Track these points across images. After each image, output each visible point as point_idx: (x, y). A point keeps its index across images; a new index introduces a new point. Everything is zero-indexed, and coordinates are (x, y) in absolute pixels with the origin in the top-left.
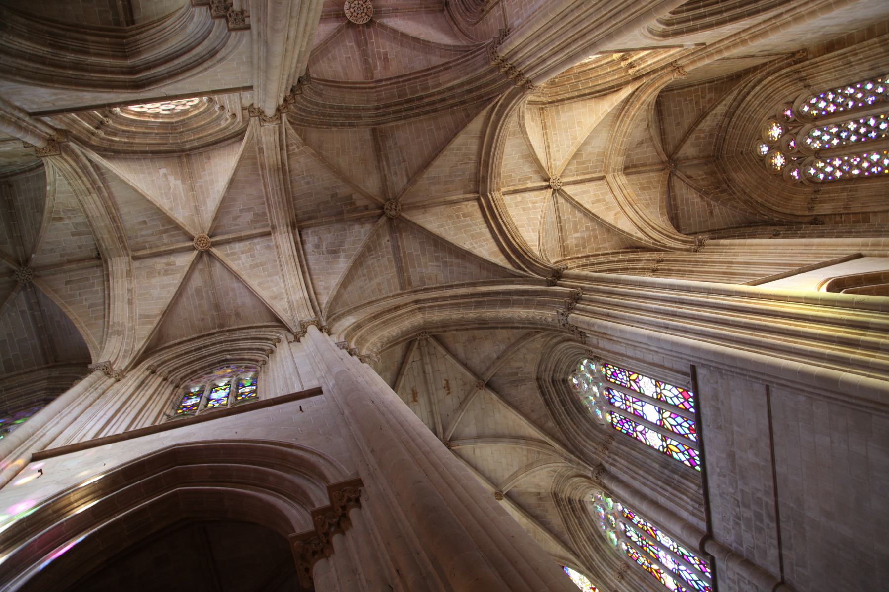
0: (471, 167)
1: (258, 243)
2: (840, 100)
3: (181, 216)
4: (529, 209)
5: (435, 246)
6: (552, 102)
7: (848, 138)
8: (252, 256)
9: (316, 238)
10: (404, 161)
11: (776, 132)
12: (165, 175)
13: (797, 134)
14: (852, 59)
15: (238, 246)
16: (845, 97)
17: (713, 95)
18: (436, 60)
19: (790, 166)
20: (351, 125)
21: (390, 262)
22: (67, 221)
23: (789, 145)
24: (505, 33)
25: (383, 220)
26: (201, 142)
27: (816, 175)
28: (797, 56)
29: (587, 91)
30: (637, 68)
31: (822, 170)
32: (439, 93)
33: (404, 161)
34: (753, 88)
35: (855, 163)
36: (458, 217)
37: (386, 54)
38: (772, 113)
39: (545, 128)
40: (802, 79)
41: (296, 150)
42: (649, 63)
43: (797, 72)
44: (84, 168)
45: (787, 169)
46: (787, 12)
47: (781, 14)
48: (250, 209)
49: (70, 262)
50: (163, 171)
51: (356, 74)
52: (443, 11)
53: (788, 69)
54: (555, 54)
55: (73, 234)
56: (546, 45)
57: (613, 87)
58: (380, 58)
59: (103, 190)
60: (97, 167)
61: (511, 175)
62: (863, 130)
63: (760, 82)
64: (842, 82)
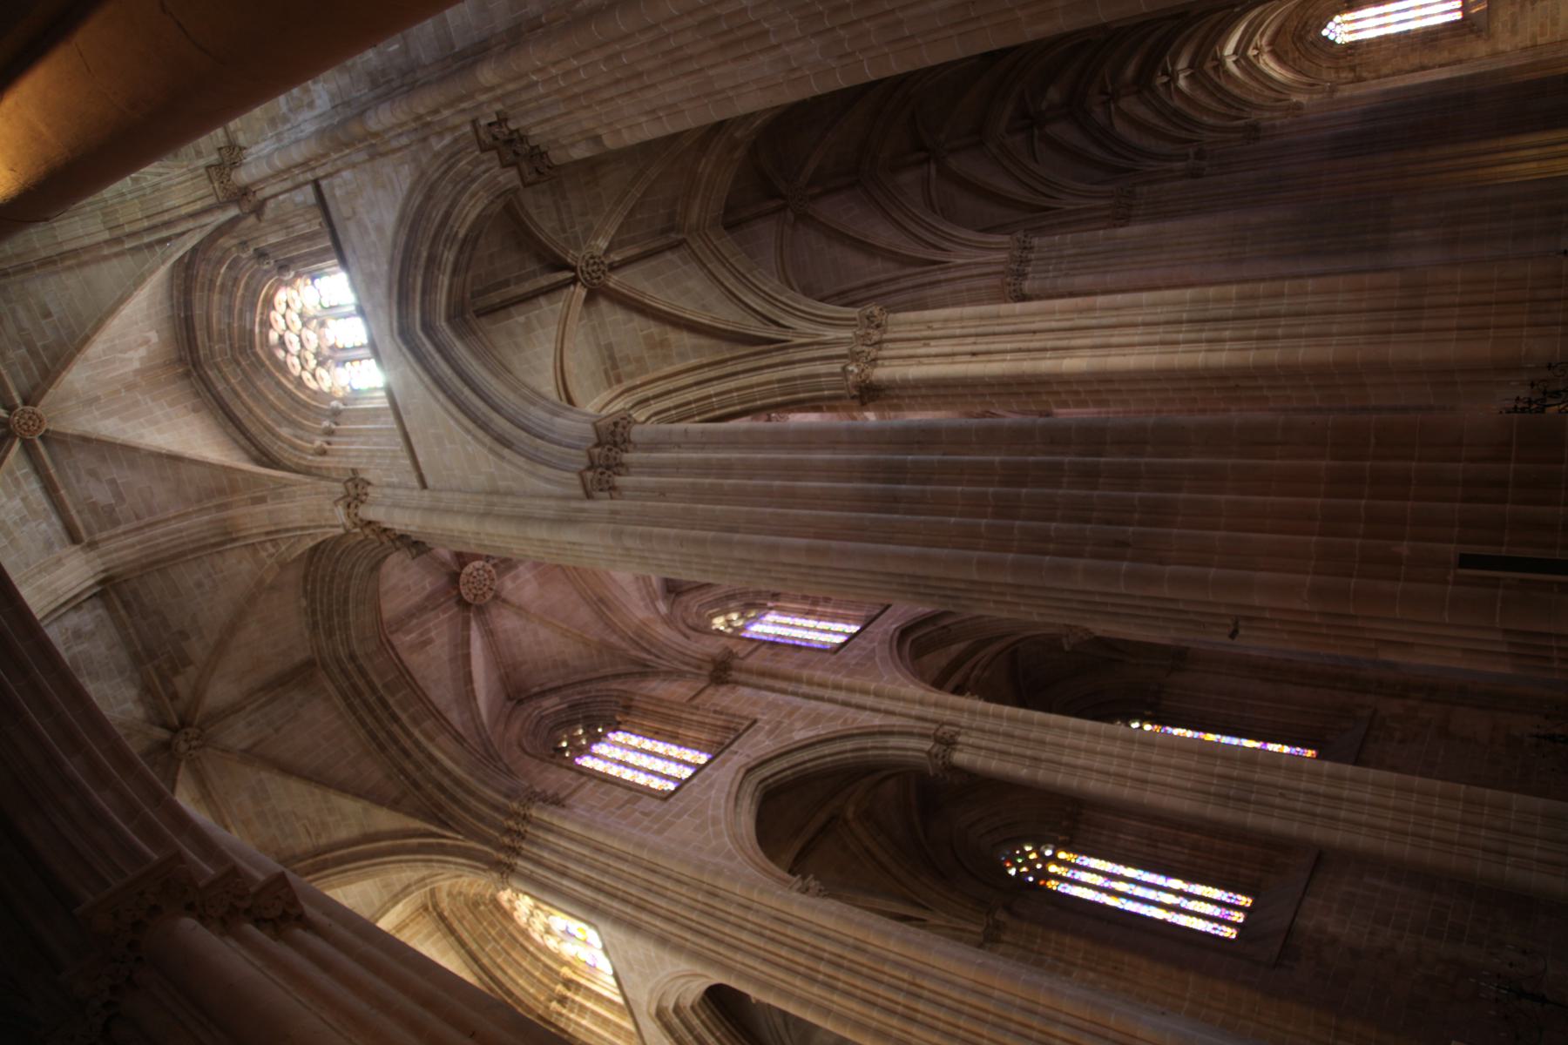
0: (305, 843)
1: (51, 525)
3: (77, 377)
6: (442, 917)
8: (24, 520)
9: (90, 627)
12: (147, 342)
15: (33, 488)
18: (454, 716)
20: (314, 626)
24: (557, 802)
25: (161, 734)
26: (227, 396)
29: (485, 961)
30: (564, 1011)
32: (417, 743)
33: (277, 730)
37: (429, 642)
41: (264, 554)
42: (584, 1022)
48: (119, 496)
50: (154, 337)
51: (391, 607)
52: (509, 698)
54: (585, 884)
56: (592, 867)
58: (421, 635)
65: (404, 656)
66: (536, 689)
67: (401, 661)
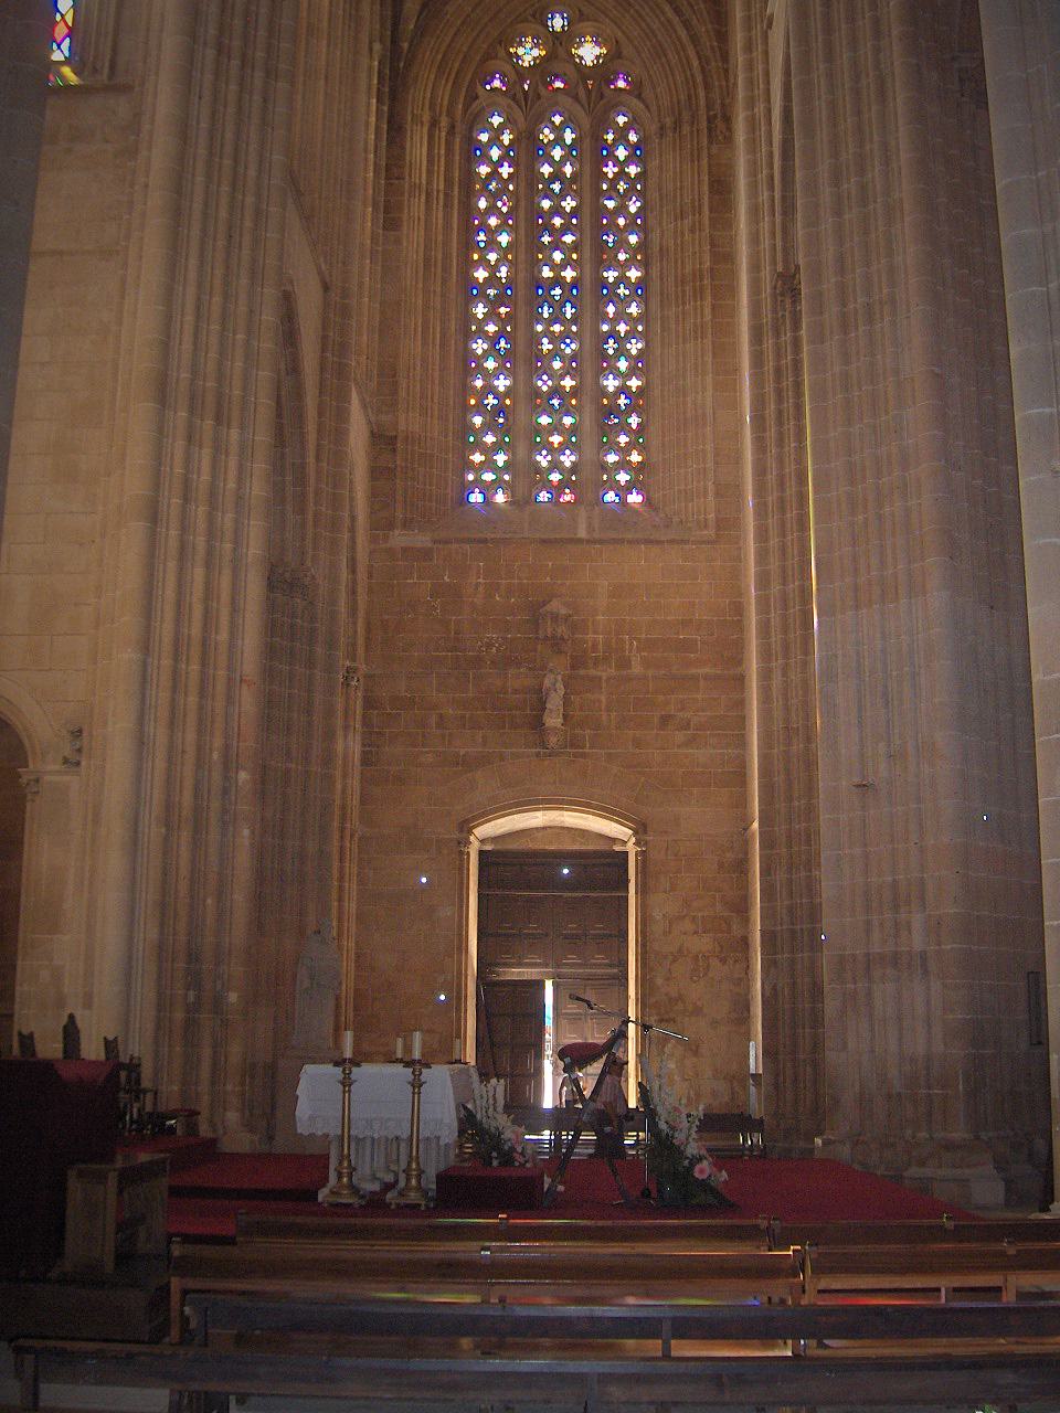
2: (622, 186)
7: (549, 194)
11: (589, 52)
13: (576, 98)
14: (687, 222)
16: (626, 196)
19: (514, 76)
23: (557, 77)
27: (489, 128)
28: (720, 123)
31: (495, 140)
34: (686, 24)
35: (499, 204)
38: (627, 50)
40: (677, 125)
43: (694, 120)
45: (507, 68)
46: (772, 200)
47: (771, 188)
53: (702, 102)
62: (557, 221)
63: (695, 40)
64: (654, 195)
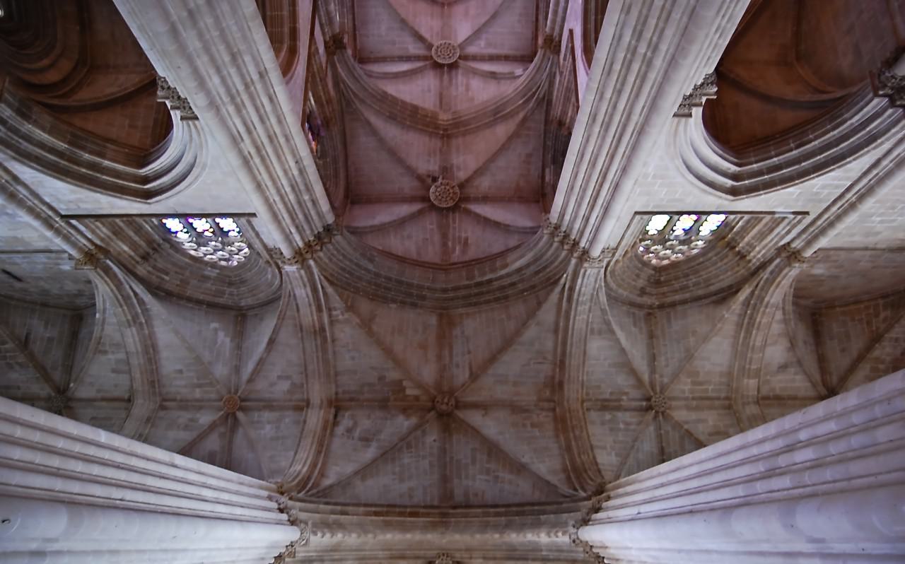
4: (620, 430)
5: (489, 455)
6: (661, 307)
8: (278, 428)
10: (469, 352)
12: (216, 330)
17: (888, 313)
20: (414, 305)
21: (431, 465)
22: (110, 356)
29: (701, 292)
32: (508, 275)
33: (469, 352)
36: (524, 425)
37: (467, 239)
39: (651, 336)
41: (341, 317)
44: (126, 298)
48: (288, 378)
49: (103, 399)
50: (214, 325)
51: (432, 254)
55: (114, 371)
57: (730, 287)
58: (460, 243)
59: (145, 325)
60: (141, 302)
61: (599, 387)
65: (467, 258)
66: (540, 181)
67: (466, 262)
